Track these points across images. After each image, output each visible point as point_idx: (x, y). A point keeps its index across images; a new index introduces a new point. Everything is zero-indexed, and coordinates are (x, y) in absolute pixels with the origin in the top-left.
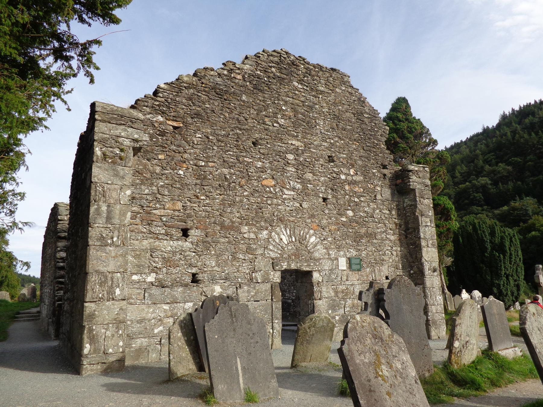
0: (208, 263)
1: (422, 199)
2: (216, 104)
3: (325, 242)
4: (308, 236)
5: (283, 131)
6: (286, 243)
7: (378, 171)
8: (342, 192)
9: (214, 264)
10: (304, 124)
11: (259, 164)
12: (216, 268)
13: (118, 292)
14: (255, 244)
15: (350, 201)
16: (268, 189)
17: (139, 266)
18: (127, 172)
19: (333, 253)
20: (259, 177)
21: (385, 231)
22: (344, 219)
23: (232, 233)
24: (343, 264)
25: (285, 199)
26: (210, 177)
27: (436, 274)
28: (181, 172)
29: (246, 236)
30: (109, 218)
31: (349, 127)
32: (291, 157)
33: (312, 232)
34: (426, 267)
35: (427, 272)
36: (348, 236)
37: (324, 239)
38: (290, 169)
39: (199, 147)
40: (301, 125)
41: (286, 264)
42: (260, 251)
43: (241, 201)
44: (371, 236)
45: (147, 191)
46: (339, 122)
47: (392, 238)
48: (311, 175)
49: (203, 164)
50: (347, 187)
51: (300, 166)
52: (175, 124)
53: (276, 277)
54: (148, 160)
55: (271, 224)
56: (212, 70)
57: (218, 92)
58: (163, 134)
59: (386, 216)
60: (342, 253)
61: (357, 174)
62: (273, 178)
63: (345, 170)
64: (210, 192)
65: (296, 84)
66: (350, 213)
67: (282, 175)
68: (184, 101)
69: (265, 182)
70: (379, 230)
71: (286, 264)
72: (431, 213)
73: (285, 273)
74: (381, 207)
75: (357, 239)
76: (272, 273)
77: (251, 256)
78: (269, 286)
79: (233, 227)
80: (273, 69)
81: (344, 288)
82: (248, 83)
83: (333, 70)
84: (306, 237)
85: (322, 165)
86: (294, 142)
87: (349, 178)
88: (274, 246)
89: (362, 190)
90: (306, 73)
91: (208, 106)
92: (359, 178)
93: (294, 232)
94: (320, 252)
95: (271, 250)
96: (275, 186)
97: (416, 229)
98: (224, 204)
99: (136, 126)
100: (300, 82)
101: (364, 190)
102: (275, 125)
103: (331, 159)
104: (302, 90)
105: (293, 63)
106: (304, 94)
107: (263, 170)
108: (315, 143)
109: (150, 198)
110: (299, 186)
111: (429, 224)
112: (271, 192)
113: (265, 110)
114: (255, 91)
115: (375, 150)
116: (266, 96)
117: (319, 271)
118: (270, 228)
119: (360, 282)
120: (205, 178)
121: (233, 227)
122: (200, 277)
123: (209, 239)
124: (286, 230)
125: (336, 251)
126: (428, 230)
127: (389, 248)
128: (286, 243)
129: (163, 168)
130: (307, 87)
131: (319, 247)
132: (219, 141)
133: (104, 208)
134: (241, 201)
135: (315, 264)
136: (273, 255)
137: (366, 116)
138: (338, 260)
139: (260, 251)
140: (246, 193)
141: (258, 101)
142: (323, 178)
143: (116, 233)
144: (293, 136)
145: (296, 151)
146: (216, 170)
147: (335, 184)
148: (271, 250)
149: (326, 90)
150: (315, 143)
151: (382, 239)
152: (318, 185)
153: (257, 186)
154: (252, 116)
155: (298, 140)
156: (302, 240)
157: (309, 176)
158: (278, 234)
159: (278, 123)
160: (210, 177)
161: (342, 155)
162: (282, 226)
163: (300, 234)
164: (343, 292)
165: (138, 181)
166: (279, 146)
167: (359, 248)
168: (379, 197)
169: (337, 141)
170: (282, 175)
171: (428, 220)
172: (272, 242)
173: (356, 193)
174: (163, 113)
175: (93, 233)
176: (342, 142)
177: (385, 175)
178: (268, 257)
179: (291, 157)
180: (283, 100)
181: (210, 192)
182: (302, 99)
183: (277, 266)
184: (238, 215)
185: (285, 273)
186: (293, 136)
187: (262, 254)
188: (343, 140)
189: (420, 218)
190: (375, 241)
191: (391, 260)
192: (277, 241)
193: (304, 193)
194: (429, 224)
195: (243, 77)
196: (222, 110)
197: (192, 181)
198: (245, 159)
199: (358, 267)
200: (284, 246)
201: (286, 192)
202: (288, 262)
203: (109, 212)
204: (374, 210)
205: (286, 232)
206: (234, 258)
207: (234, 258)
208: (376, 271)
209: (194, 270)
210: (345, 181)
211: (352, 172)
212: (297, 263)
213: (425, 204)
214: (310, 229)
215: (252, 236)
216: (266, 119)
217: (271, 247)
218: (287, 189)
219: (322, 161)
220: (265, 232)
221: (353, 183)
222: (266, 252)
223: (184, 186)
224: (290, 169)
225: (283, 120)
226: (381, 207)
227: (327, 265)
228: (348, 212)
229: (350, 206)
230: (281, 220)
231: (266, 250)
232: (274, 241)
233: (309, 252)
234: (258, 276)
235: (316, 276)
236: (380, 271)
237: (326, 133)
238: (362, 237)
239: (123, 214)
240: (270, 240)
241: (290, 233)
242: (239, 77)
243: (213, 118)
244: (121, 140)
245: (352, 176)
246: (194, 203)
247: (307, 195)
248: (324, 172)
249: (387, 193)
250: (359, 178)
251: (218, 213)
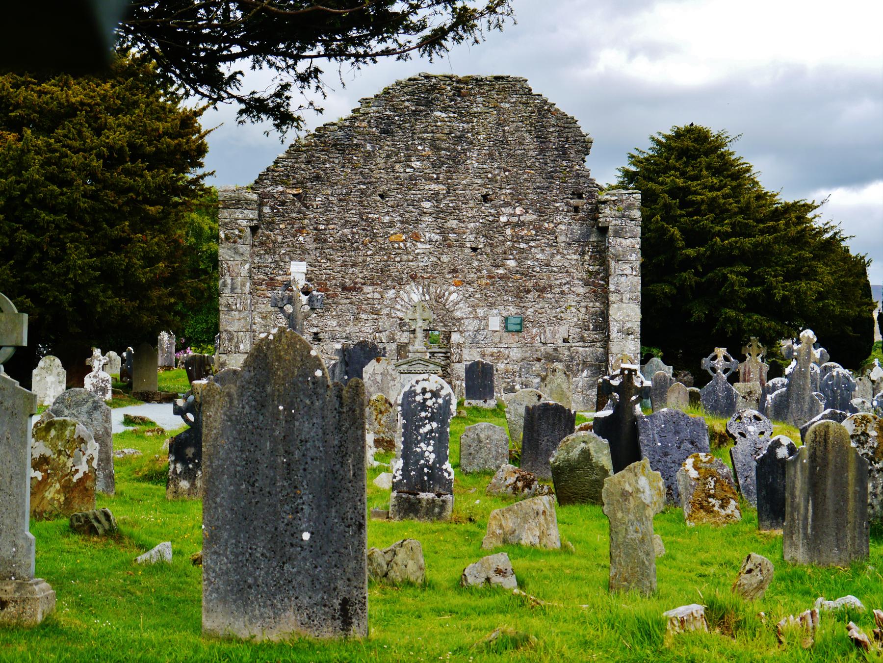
0: (329, 323)
1: (619, 240)
2: (337, 161)
3: (472, 299)
4: (446, 294)
5: (419, 176)
7: (567, 204)
8: (501, 238)
9: (335, 323)
10: (449, 160)
11: (386, 219)
12: (338, 328)
13: (242, 346)
14: (379, 304)
15: (512, 248)
16: (396, 245)
17: (265, 326)
18: (245, 249)
20: (387, 233)
21: (567, 283)
22: (501, 271)
23: (354, 293)
24: (495, 323)
25: (418, 254)
26: (331, 239)
27: (632, 337)
28: (301, 239)
29: (369, 296)
30: (233, 289)
31: (519, 152)
34: (614, 328)
35: (614, 334)
36: (506, 291)
38: (427, 219)
39: (320, 210)
40: (443, 163)
42: (385, 311)
43: (364, 261)
44: (543, 290)
45: (270, 260)
46: (504, 148)
47: (581, 290)
48: (456, 222)
49: (323, 227)
50: (509, 232)
51: (439, 214)
52: (295, 192)
54: (271, 231)
55: (400, 281)
56: (334, 124)
57: (339, 147)
58: (283, 203)
59: (573, 262)
60: (495, 311)
61: (527, 212)
62: (404, 233)
63: (508, 210)
64: (331, 255)
65: (438, 114)
66: (511, 263)
67: (415, 227)
68: (303, 166)
69: (393, 238)
70: (558, 282)
72: (636, 258)
74: (565, 252)
75: (520, 294)
76: (399, 334)
77: (375, 317)
78: (394, 346)
79: (355, 288)
80: (407, 104)
81: (495, 350)
82: (374, 129)
83: (497, 78)
85: (472, 208)
86: (433, 186)
87: (515, 219)
89: (533, 232)
90: (454, 95)
91: (328, 166)
92: (531, 217)
93: (428, 290)
96: (405, 240)
98: (345, 266)
99: (251, 207)
100: (445, 110)
101: (537, 232)
102: (408, 170)
103: (485, 198)
104: (446, 119)
105: (434, 87)
106: (449, 124)
107: (391, 224)
108: (464, 182)
109: (273, 266)
110: (437, 237)
111: (628, 272)
112: (400, 248)
113: (397, 155)
114: (383, 135)
115: (561, 175)
116: (396, 138)
117: (461, 333)
118: (398, 287)
119: (519, 345)
120: (325, 241)
121: (355, 288)
122: (321, 336)
123: (330, 301)
124: (418, 289)
126: (626, 279)
127: (574, 304)
129: (285, 237)
130: (454, 113)
132: (340, 200)
133: (229, 281)
134: (364, 261)
135: (454, 325)
137: (552, 130)
139: (385, 311)
140: (369, 253)
141: (386, 148)
142: (472, 225)
143: (239, 301)
144: (431, 179)
145: (435, 197)
146: (336, 231)
147: (491, 229)
149: (485, 110)
150: (464, 182)
151: (563, 292)
152: (465, 233)
153: (384, 243)
154: (379, 166)
155: (438, 183)
156: (438, 297)
157: (453, 223)
159: (412, 168)
160: (331, 239)
161: (504, 191)
162: (413, 284)
164: (492, 355)
165: (262, 252)
166: (414, 194)
167: (522, 305)
168: (562, 238)
169: (498, 175)
170: (415, 227)
171: (627, 266)
173: (522, 237)
174: (283, 183)
175: (222, 301)
176: (507, 173)
177: (576, 209)
179: (427, 205)
180: (419, 138)
181: (331, 255)
182: (446, 131)
184: (360, 275)
186: (431, 179)
187: (388, 315)
188: (508, 171)
189: (613, 263)
190: (549, 296)
191: (575, 319)
193: (446, 243)
194: (628, 272)
195: (369, 122)
196: (343, 167)
197: (311, 245)
198: (370, 216)
199: (518, 327)
201: (419, 245)
203: (233, 284)
204: (553, 255)
206: (357, 319)
207: (357, 319)
208: (548, 332)
209: (315, 330)
210: (508, 223)
211: (518, 210)
215: (377, 296)
216: (398, 166)
217: (399, 307)
218: (421, 242)
219: (472, 204)
220: (393, 291)
221: (521, 224)
223: (305, 251)
224: (427, 219)
225: (418, 163)
226: (565, 252)
227: (471, 325)
228: (508, 262)
229: (512, 254)
230: (413, 278)
232: (402, 300)
236: (554, 334)
237: (481, 166)
238: (528, 291)
239: (243, 285)
242: (365, 124)
243: (334, 179)
244: (239, 221)
245: (520, 216)
246: (315, 267)
247: (450, 246)
248: (474, 217)
250: (531, 217)
251: (340, 275)
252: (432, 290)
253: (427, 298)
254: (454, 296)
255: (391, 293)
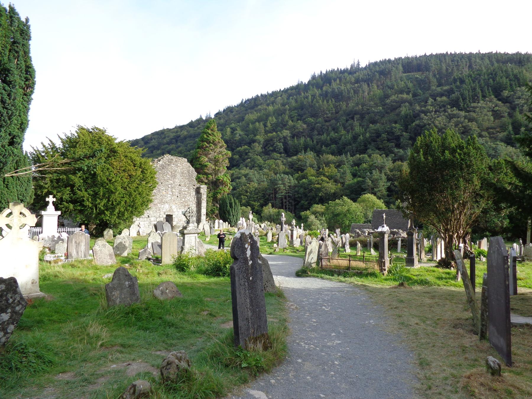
10: (174, 176)
32: (170, 186)
34: (202, 214)
51: (172, 188)
53: (165, 216)
73: (167, 215)
92: (187, 190)
94: (175, 210)
97: (201, 204)
100: (174, 164)
107: (163, 190)
126: (204, 204)
145: (171, 184)
157: (174, 190)
166: (167, 183)
179: (170, 186)
185: (167, 215)
193: (173, 195)
213: (204, 197)
221: (185, 191)
234: (161, 216)
235: (174, 216)
249: (194, 193)
250: (187, 190)
255: (163, 206)
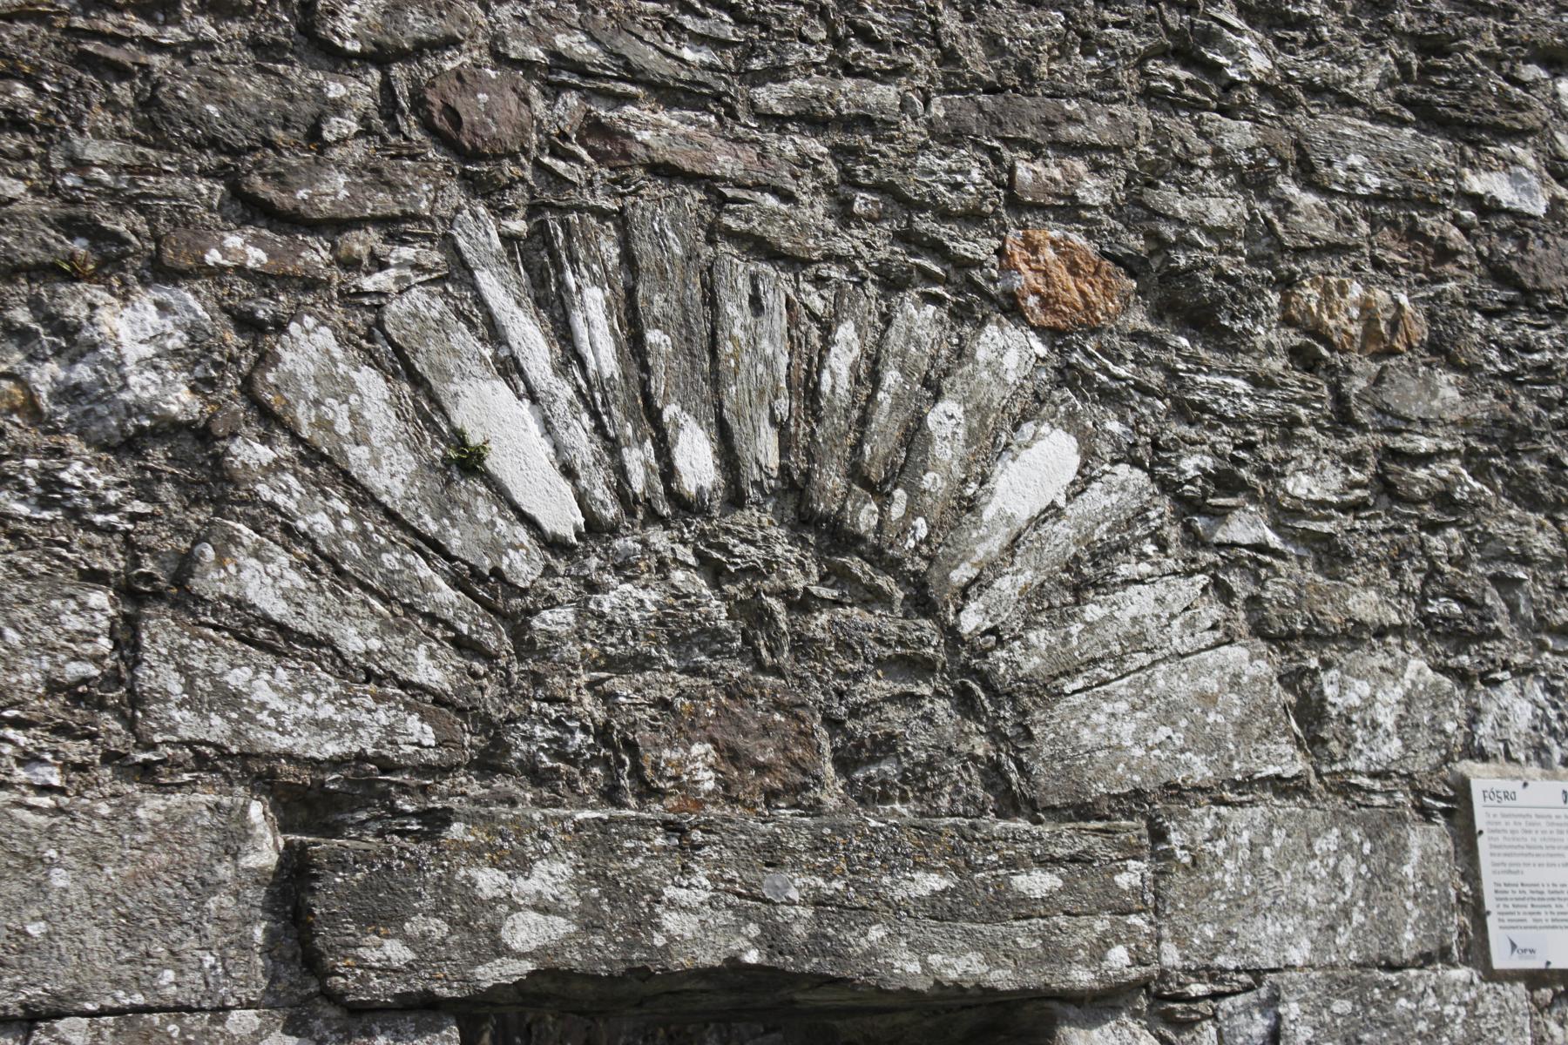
4: (946, 419)
6: (563, 518)
19: (1382, 694)
33: (1009, 351)
37: (1225, 481)
41: (550, 876)
71: (550, 876)
84: (914, 435)
88: (324, 564)
93: (707, 347)
95: (276, 640)
125: (1418, 669)
128: (563, 518)
131: (1138, 603)
136: (297, 718)
138: (1457, 810)
148: (276, 640)
158: (398, 363)
162: (481, 234)
163: (809, 393)
172: (286, 493)
178: (205, 760)
183: (385, 919)
192: (392, 472)
200: (523, 565)
202: (596, 844)
205: (563, 335)
212: (773, 855)
214: (975, 300)
217: (265, 582)
222: (158, 675)
231: (161, 630)
232: (323, 465)
233: (972, 681)
240: (249, 452)
241: (634, 346)
252: (759, 343)
253: (697, 463)
254: (1041, 467)
